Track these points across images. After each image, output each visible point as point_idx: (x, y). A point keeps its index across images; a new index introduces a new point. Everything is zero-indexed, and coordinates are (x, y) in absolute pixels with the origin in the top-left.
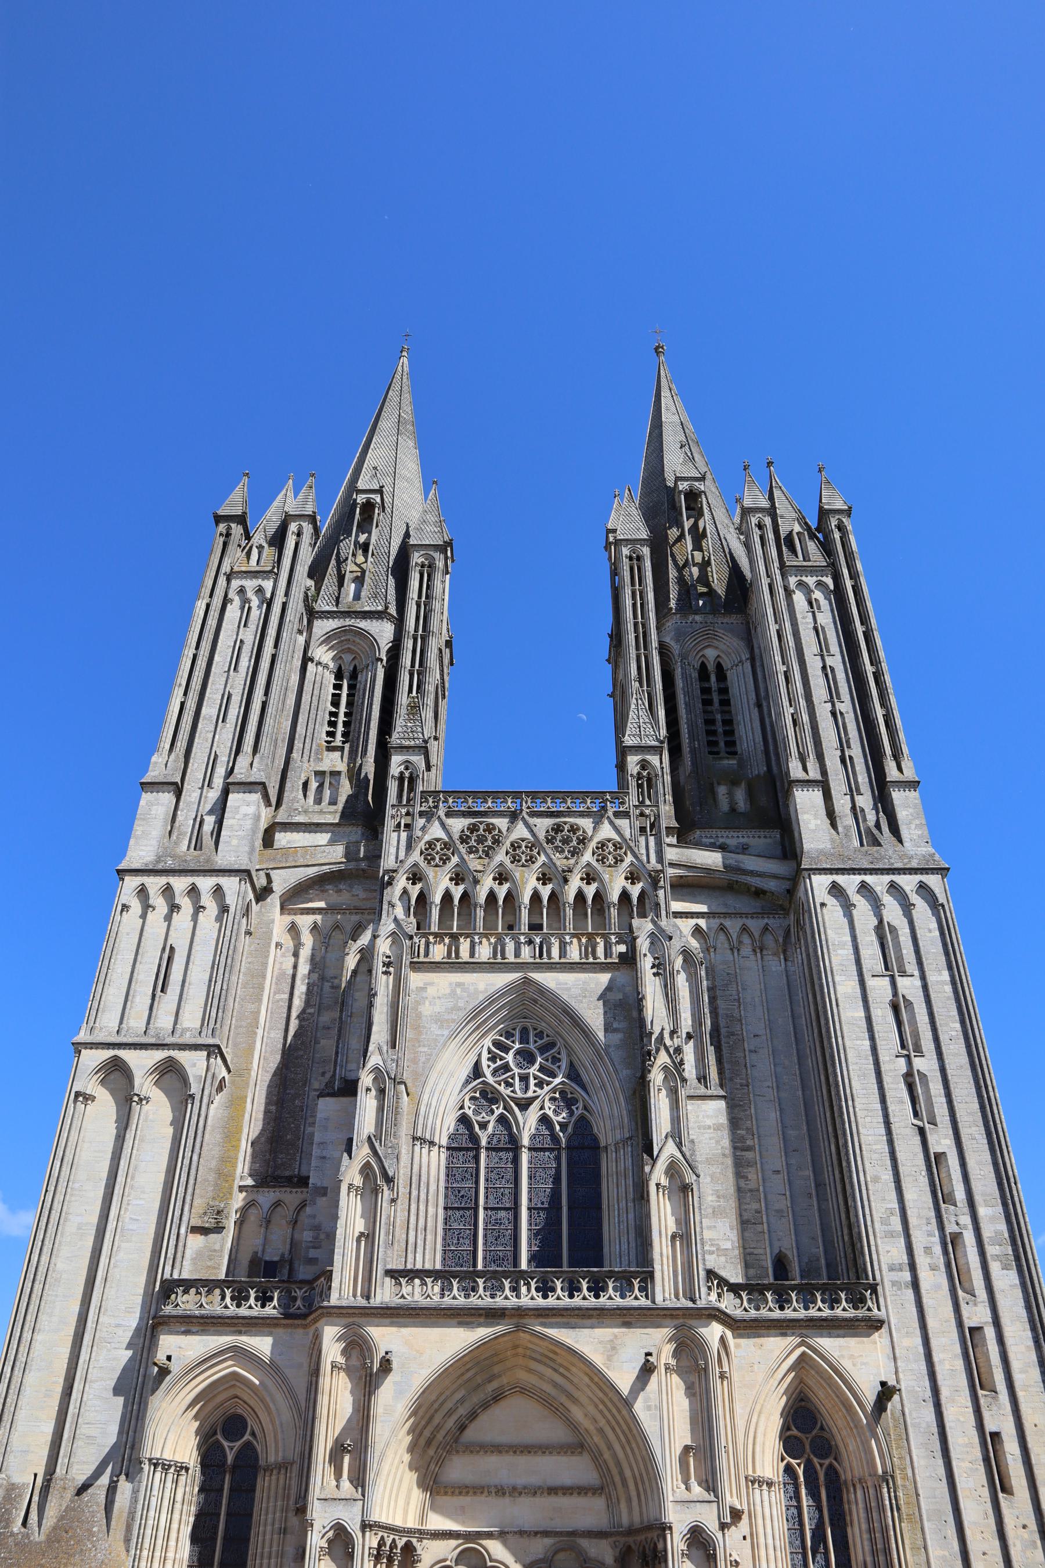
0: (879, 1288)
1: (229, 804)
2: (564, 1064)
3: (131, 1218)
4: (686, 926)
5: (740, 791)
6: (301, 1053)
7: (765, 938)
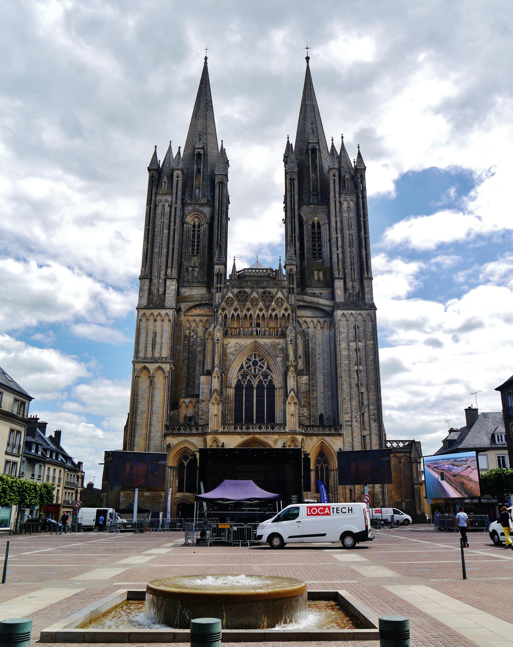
0: (342, 427)
1: (167, 285)
2: (266, 365)
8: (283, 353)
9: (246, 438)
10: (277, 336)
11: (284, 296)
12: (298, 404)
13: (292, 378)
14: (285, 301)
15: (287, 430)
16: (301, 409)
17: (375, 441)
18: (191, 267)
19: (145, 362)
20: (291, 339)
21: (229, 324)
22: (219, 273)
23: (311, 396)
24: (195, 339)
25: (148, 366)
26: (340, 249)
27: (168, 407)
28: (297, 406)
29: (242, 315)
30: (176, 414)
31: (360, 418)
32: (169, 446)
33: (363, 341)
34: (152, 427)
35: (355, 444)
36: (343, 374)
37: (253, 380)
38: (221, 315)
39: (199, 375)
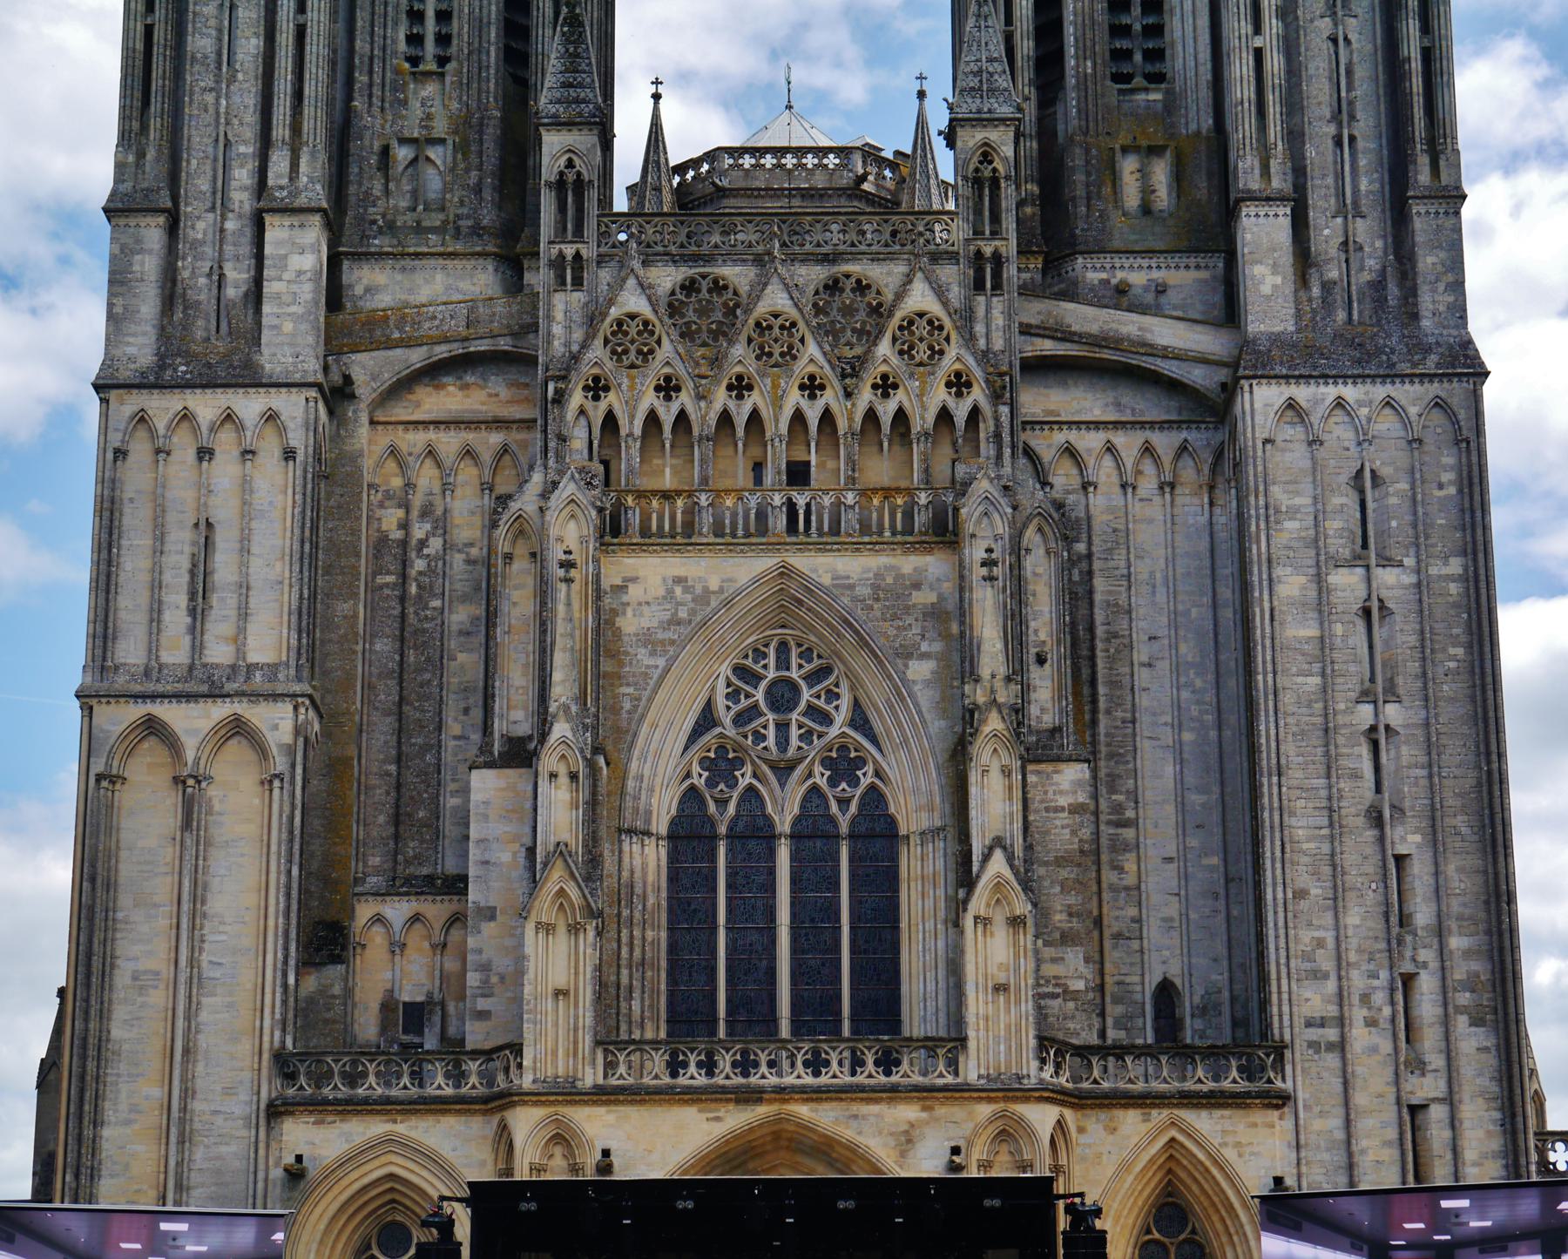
0: (1288, 1054)
1: (268, 250)
2: (845, 702)
3: (211, 962)
4: (1050, 446)
5: (1163, 165)
6: (427, 676)
7: (1180, 464)
8: (945, 636)
9: (735, 1119)
10: (908, 538)
11: (945, 304)
12: (1030, 922)
13: (996, 781)
14: (954, 336)
15: (972, 1071)
16: (1048, 952)
17: (1480, 1133)
18: (403, 141)
19: (154, 697)
20: (990, 550)
21: (631, 471)
22: (571, 177)
23: (1109, 876)
24: (436, 559)
25: (172, 714)
26: (1272, 25)
27: (286, 949)
28: (1027, 939)
29: (704, 417)
30: (337, 990)
31: (1393, 1003)
32: (296, 1174)
33: (1409, 561)
34: (200, 1068)
35: (1363, 1152)
36: (1289, 748)
37: (771, 792)
38: (583, 421)
39: (463, 768)
